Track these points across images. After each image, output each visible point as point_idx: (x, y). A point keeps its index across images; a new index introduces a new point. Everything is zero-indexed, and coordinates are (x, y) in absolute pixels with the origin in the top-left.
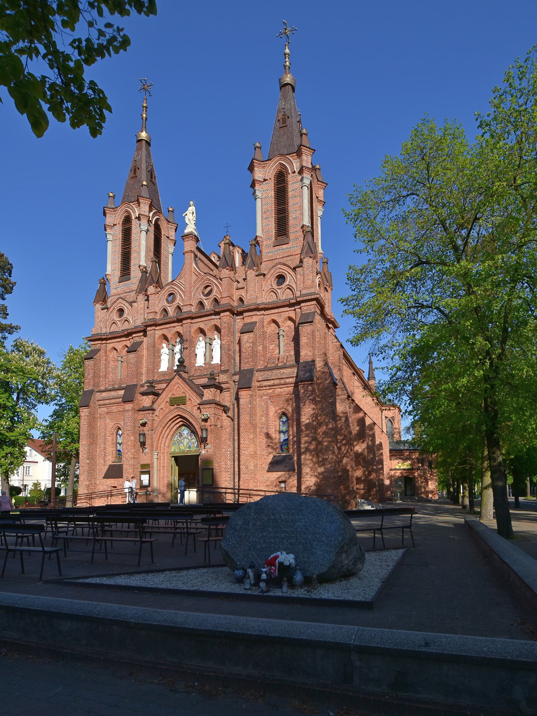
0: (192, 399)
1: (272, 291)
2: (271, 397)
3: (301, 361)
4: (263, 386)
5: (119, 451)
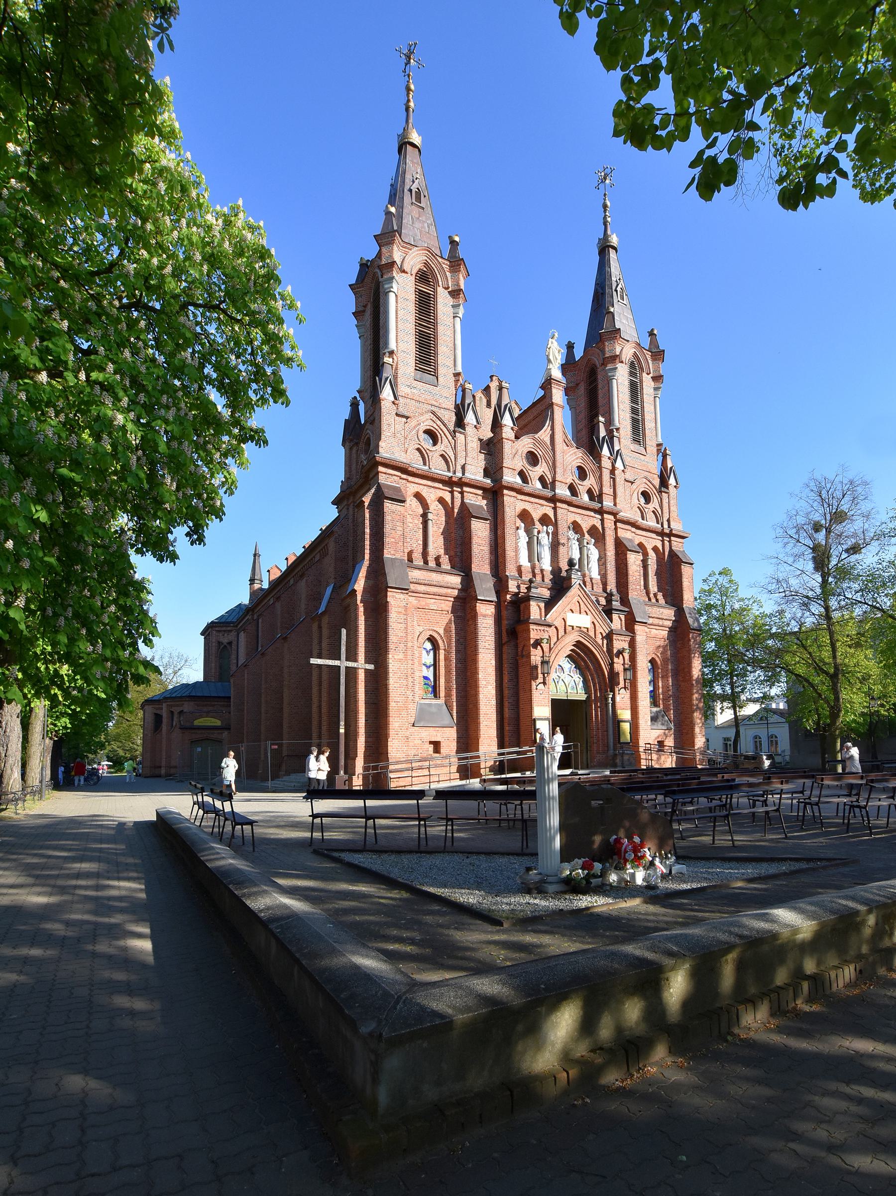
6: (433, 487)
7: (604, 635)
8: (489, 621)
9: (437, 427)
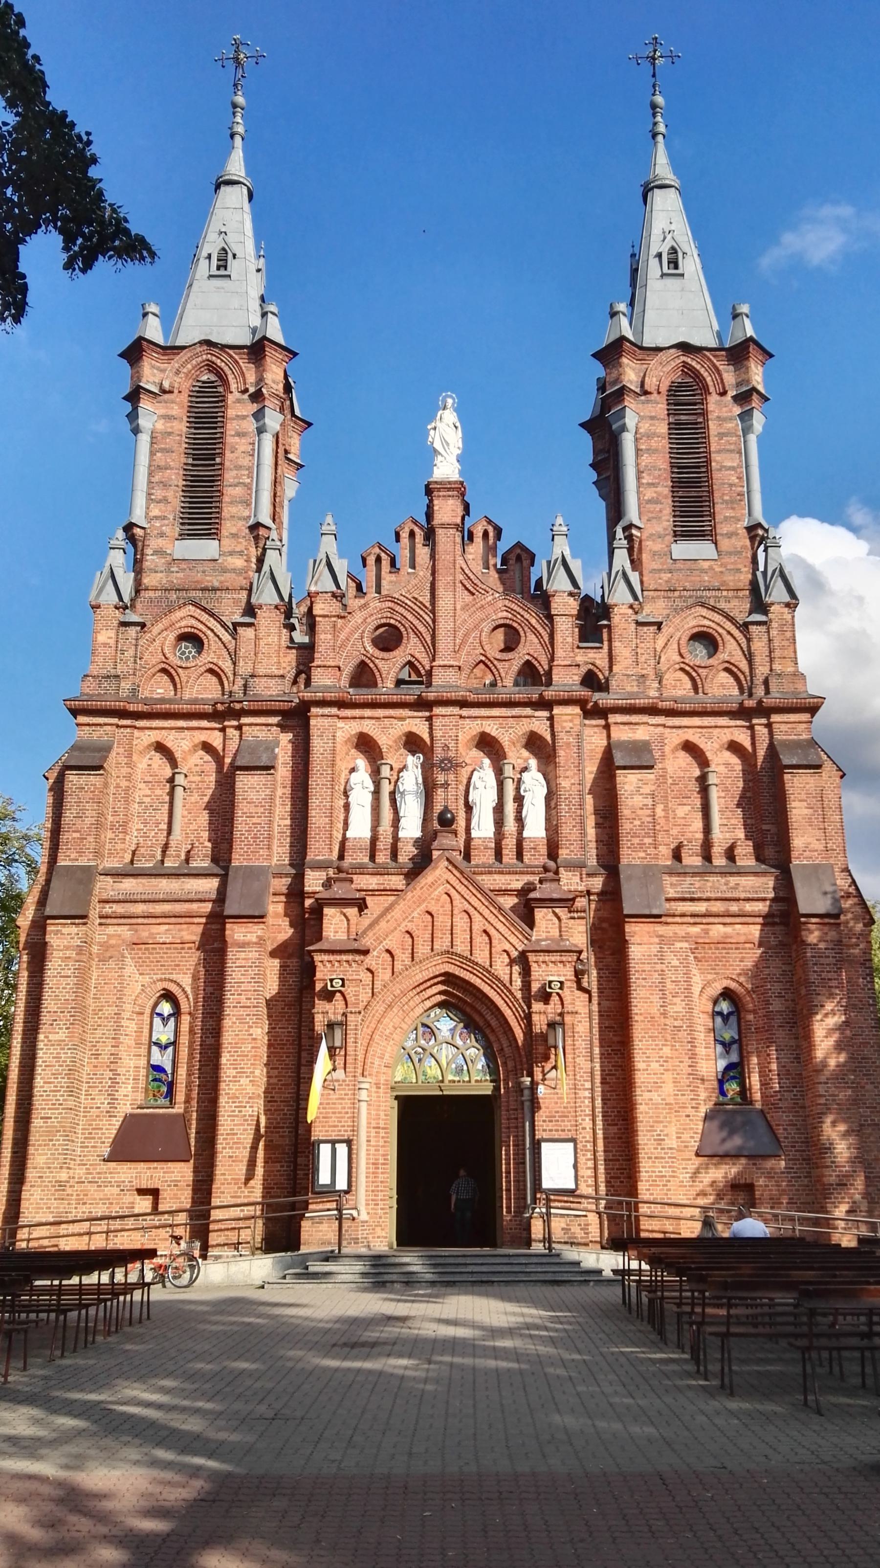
0: (492, 932)
1: (682, 669)
2: (697, 945)
3: (795, 862)
4: (677, 913)
5: (158, 1069)
6: (188, 729)
7: (514, 954)
8: (250, 955)
9: (201, 626)
